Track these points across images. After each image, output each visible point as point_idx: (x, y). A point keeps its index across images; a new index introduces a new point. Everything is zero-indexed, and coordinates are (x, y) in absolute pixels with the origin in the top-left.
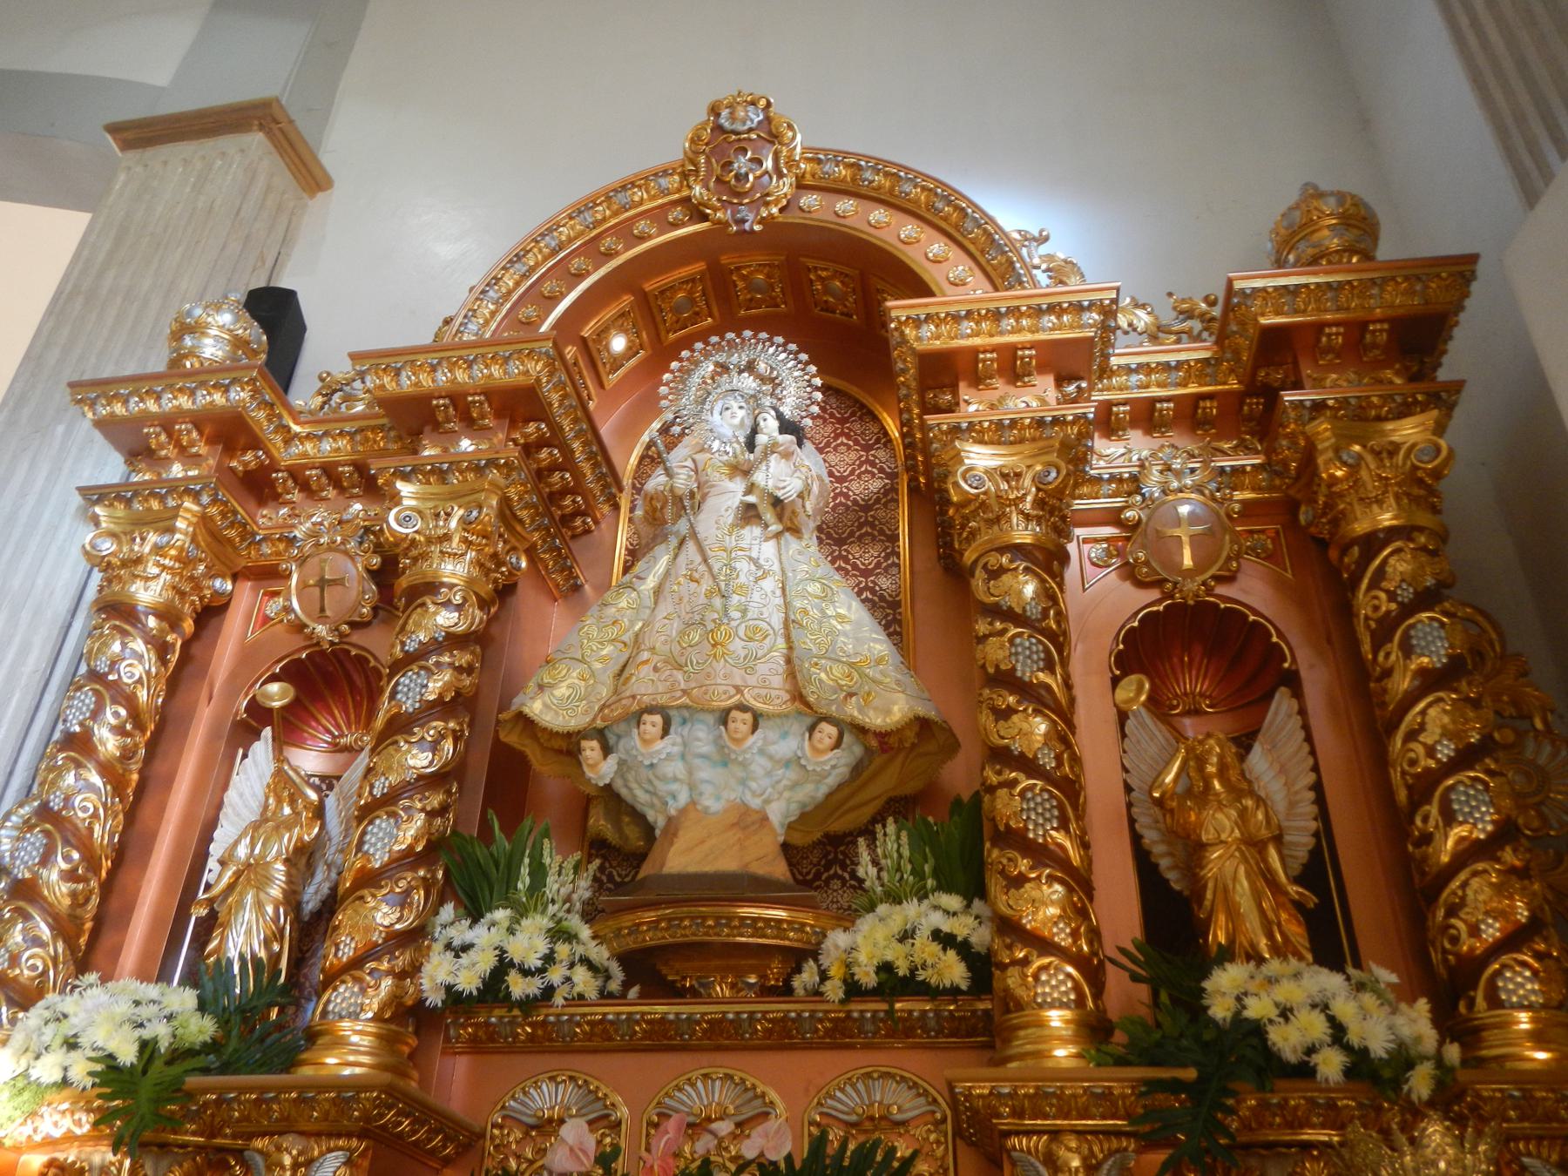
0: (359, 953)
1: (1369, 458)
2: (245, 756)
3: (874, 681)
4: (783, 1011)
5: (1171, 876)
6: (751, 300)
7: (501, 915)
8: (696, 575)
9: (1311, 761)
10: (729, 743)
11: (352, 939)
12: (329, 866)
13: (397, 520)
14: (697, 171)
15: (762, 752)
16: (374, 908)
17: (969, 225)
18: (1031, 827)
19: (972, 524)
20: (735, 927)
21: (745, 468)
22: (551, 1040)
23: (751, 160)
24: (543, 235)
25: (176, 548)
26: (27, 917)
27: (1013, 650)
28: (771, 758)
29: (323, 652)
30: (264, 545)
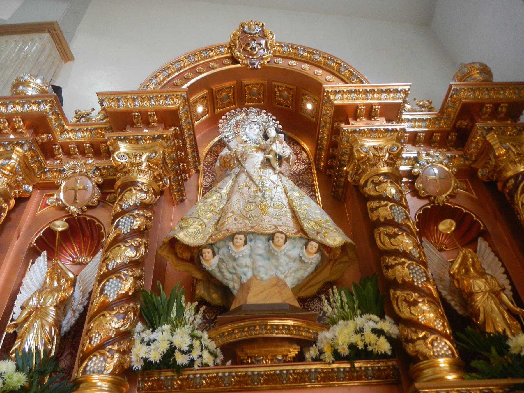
0: (102, 342)
1: (512, 148)
2: (33, 263)
3: (326, 228)
4: (302, 369)
5: (457, 308)
6: (251, 99)
7: (166, 327)
9: (500, 264)
11: (99, 334)
12: (74, 311)
13: (118, 156)
14: (236, 46)
17: (342, 69)
18: (415, 280)
19: (364, 167)
20: (280, 330)
21: (263, 148)
22: (190, 387)
23: (257, 43)
24: (175, 63)
25: (11, 167)
28: (289, 257)
29: (74, 218)
30: (48, 173)
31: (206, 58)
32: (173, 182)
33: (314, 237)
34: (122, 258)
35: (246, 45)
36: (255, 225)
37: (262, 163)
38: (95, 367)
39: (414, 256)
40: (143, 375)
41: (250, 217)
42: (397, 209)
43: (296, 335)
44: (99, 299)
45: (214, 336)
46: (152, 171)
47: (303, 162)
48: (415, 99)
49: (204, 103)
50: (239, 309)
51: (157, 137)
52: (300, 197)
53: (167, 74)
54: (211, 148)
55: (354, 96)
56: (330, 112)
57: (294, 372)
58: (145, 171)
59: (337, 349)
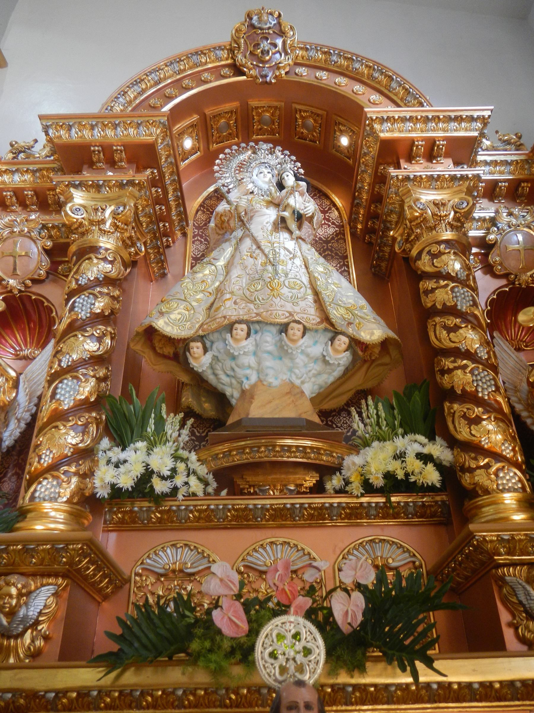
0: (55, 461)
3: (361, 317)
6: (260, 129)
7: (141, 445)
10: (288, 343)
11: (51, 452)
12: (19, 420)
13: (71, 210)
14: (239, 47)
15: (303, 352)
16: (65, 433)
17: (394, 85)
18: (480, 390)
19: (418, 231)
20: (294, 452)
21: (276, 202)
22: (172, 522)
23: (271, 44)
24: (151, 73)
27: (454, 294)
28: (308, 355)
29: (14, 296)
31: (196, 65)
32: (150, 248)
33: (344, 329)
34: (79, 352)
35: (254, 46)
36: (262, 311)
37: (274, 223)
38: (47, 493)
39: (481, 358)
40: (111, 504)
41: (255, 301)
42: (462, 291)
43: (314, 459)
44: (50, 406)
45: (205, 457)
46: (120, 232)
47: (333, 223)
48: (497, 132)
49: (194, 135)
50: (238, 423)
51: (127, 183)
52: (326, 274)
53: (140, 89)
54: (203, 202)
55: (409, 125)
56: (374, 150)
57: (310, 507)
58: (109, 232)
59: (369, 479)
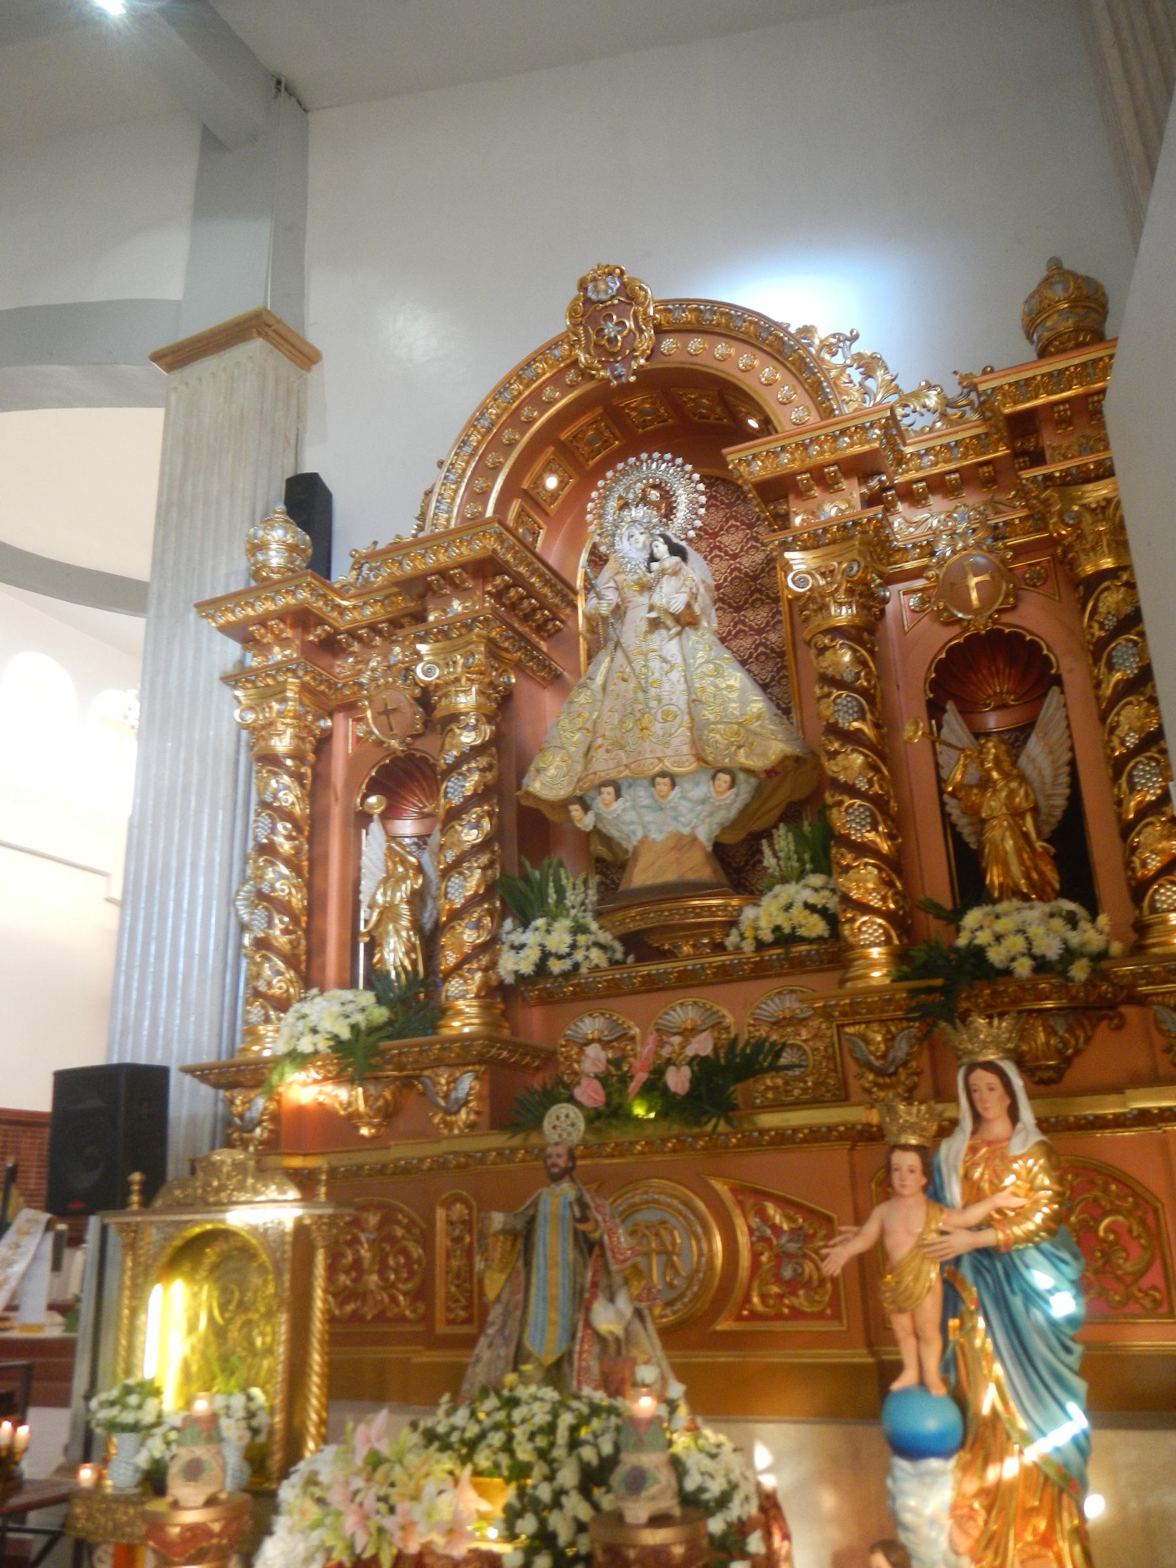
7: (540, 922)
8: (626, 677)
14: (579, 340)
24: (478, 420)
26: (269, 960)
28: (690, 800)
29: (398, 758)
